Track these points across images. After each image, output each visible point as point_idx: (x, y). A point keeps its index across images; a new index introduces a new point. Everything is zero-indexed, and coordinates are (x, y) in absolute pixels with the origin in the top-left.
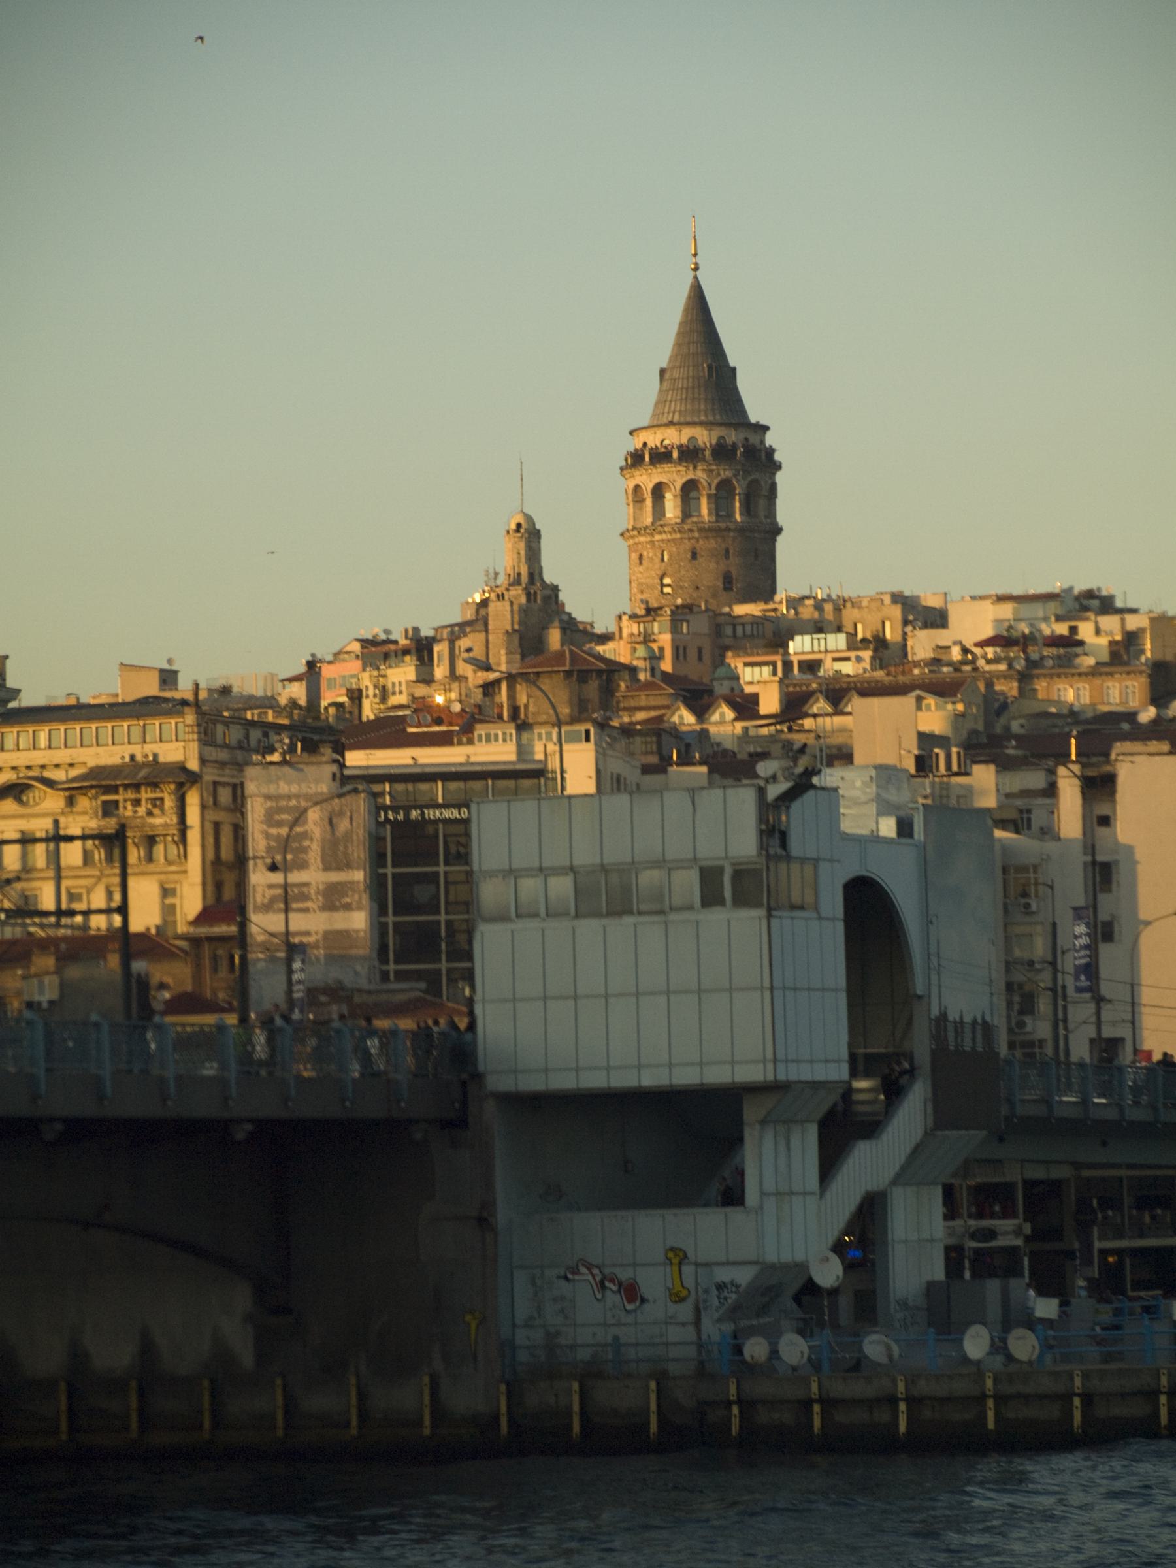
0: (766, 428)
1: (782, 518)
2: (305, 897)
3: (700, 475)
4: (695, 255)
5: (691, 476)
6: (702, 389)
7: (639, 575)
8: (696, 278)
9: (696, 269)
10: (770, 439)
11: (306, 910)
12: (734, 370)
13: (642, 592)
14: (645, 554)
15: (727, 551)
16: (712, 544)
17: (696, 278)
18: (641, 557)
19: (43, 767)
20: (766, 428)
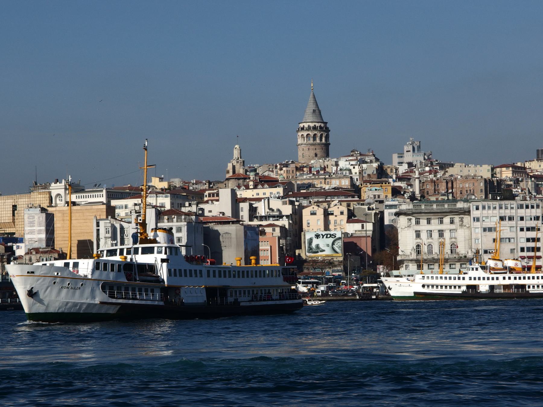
0: (327, 123)
2: (35, 232)
3: (310, 133)
5: (308, 133)
10: (328, 125)
11: (35, 234)
15: (316, 149)
16: (313, 147)
20: (327, 123)
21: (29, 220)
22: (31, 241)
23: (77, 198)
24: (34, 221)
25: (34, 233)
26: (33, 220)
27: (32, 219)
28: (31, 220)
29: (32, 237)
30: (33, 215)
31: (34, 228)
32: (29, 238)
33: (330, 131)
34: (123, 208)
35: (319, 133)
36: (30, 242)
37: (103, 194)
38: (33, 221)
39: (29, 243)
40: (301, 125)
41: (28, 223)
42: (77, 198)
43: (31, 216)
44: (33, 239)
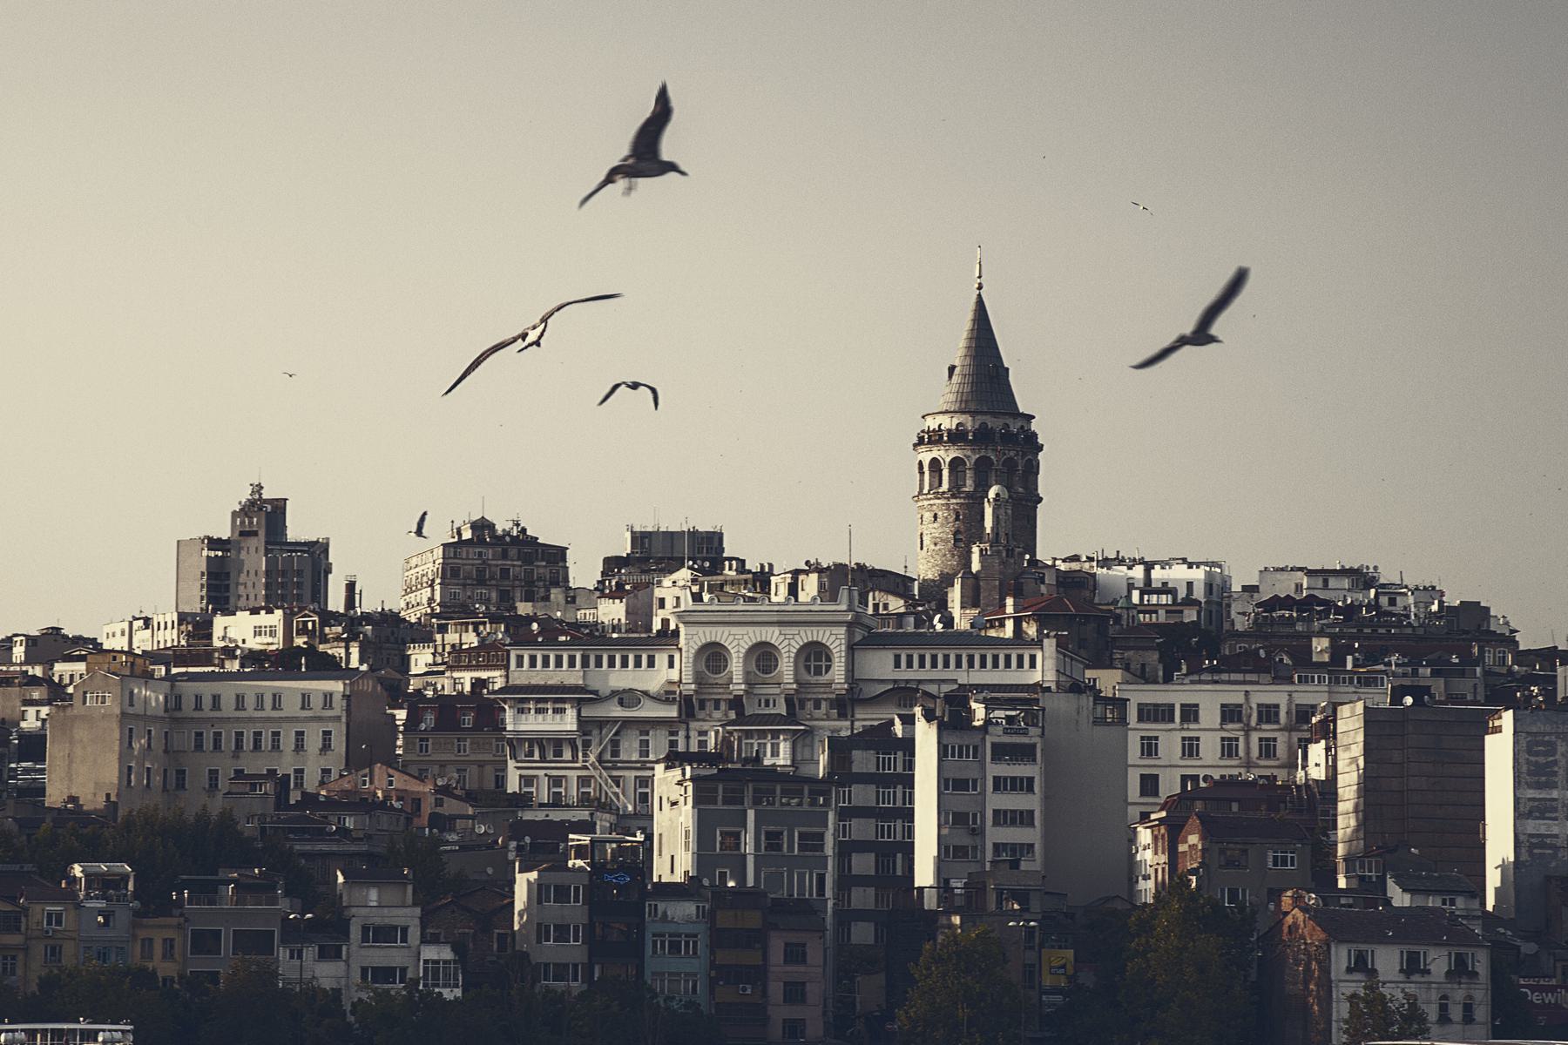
1: (1041, 491)
2: (1555, 810)
4: (980, 277)
5: (983, 453)
6: (988, 385)
7: (934, 531)
8: (979, 295)
9: (980, 287)
11: (1555, 819)
12: (1007, 369)
13: (936, 544)
14: (940, 513)
17: (979, 295)
18: (935, 517)
19: (920, 681)
20: (1033, 417)
21: (1533, 759)
22: (1543, 846)
23: (897, 665)
24: (1555, 763)
25: (1554, 815)
26: (1551, 758)
27: (1546, 754)
28: (1542, 760)
29: (1543, 831)
30: (1547, 738)
31: (1555, 794)
32: (1531, 836)
33: (1040, 448)
34: (1172, 720)
35: (1022, 459)
36: (1536, 851)
37: (1033, 659)
38: (1548, 764)
39: (1531, 853)
40: (932, 423)
41: (1529, 773)
42: (897, 665)
43: (1538, 744)
44: (1548, 841)
